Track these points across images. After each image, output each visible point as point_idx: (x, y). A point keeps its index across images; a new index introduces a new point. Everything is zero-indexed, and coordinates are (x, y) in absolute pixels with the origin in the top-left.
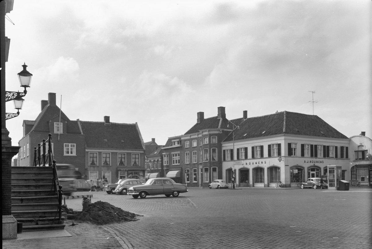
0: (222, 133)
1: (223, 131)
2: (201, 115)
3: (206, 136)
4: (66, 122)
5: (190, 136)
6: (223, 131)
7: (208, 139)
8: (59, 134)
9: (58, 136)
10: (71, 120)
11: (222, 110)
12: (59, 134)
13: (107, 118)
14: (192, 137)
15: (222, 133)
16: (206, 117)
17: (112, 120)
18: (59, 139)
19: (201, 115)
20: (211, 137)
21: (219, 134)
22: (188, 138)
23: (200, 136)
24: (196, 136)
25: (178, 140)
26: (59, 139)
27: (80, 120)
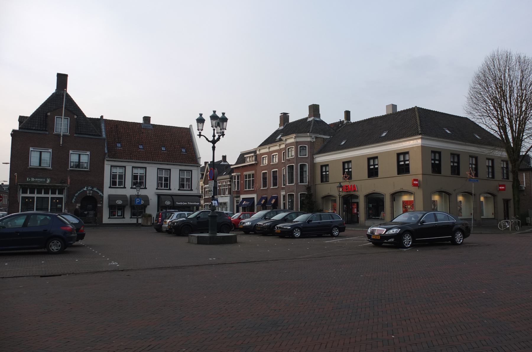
0: (314, 140)
1: (316, 138)
2: (284, 117)
3: (291, 144)
4: (75, 117)
5: (269, 148)
6: (316, 138)
7: (294, 149)
8: (62, 135)
9: (60, 137)
10: (87, 117)
11: (314, 109)
12: (62, 135)
13: (147, 119)
14: (272, 149)
15: (314, 140)
16: (291, 120)
17: (152, 122)
18: (61, 143)
19: (284, 117)
20: (299, 146)
21: (311, 142)
22: (266, 150)
23: (283, 146)
24: (277, 148)
25: (253, 154)
26: (61, 143)
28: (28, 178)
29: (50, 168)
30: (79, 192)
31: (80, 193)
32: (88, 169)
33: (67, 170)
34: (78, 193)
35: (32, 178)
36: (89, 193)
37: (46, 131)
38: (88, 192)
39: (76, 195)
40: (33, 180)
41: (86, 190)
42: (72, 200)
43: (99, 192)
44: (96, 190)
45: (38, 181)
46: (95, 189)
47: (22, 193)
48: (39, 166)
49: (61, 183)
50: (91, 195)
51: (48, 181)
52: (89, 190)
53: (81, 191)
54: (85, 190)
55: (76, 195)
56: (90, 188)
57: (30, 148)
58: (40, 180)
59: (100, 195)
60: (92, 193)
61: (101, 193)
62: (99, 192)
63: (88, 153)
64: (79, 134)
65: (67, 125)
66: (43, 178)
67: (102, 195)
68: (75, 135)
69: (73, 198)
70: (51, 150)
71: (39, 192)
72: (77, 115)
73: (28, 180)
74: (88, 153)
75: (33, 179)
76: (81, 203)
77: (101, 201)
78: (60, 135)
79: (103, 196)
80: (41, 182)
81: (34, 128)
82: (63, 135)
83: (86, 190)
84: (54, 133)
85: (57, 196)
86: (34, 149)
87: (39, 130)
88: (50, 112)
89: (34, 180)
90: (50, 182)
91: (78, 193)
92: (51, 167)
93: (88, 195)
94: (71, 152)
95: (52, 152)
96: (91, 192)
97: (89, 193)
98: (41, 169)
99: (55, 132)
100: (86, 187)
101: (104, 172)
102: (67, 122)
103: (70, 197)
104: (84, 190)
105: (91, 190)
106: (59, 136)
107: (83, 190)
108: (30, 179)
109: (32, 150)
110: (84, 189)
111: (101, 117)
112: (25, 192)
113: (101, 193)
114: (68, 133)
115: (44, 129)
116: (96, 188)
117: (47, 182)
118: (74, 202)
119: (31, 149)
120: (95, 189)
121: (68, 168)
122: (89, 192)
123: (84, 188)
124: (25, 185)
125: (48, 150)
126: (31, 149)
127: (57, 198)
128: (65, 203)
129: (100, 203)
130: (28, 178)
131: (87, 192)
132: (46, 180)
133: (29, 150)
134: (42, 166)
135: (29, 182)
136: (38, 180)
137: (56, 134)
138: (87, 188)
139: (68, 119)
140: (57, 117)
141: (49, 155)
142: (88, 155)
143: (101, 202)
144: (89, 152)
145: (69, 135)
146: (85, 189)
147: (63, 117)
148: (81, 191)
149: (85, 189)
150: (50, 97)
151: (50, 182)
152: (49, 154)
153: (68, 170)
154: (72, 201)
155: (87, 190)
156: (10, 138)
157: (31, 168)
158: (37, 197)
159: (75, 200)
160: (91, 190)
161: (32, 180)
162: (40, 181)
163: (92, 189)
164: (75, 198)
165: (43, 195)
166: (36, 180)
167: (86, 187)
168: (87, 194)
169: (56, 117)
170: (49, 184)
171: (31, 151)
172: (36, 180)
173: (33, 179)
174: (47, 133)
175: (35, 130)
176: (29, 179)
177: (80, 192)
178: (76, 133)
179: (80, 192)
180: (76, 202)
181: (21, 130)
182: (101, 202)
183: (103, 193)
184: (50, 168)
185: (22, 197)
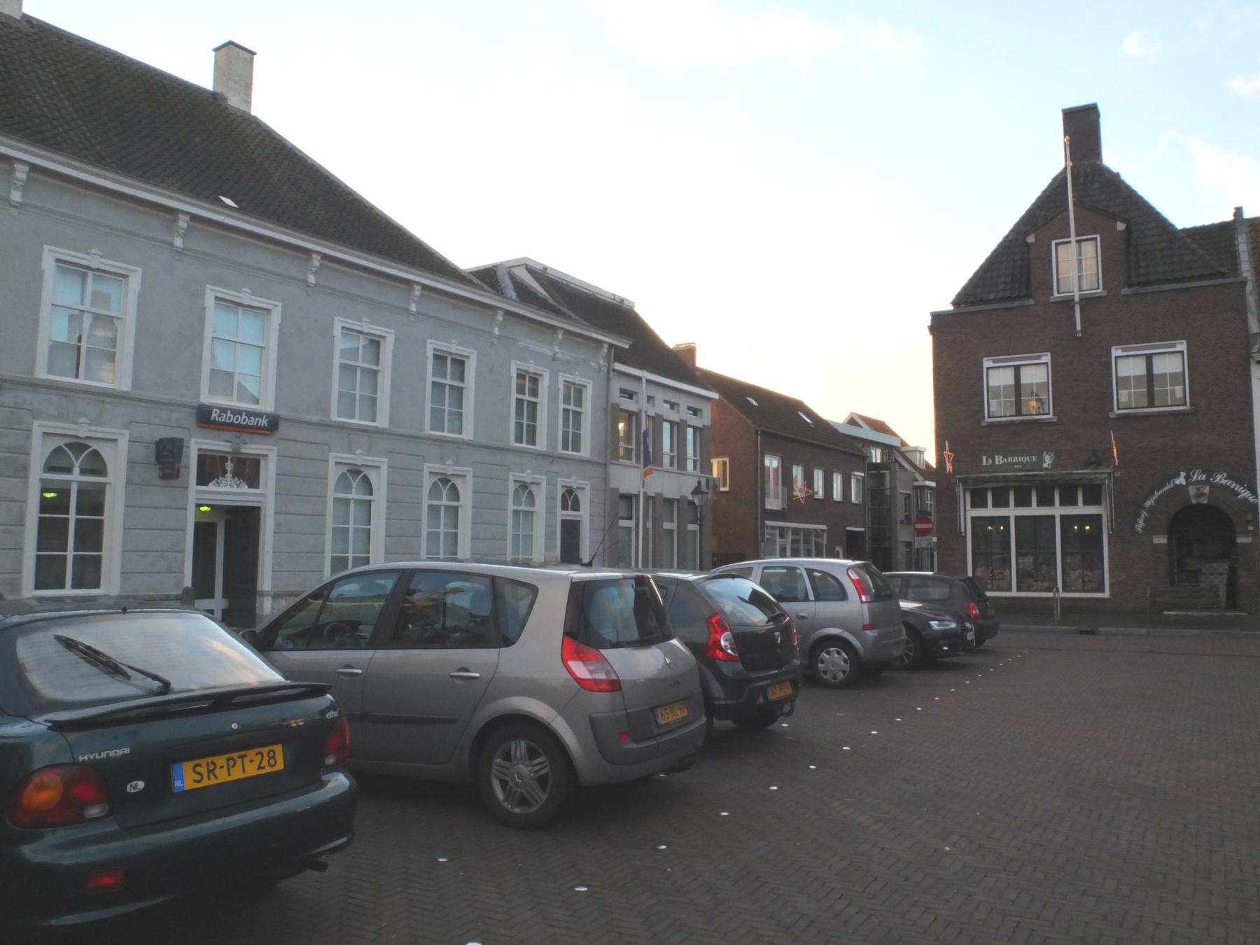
8: (1077, 299)
9: (1073, 309)
12: (1077, 299)
18: (1079, 327)
26: (1079, 327)
27: (1248, 214)
28: (984, 458)
29: (1051, 416)
30: (1157, 494)
31: (1162, 495)
32: (1185, 404)
33: (1108, 418)
34: (1154, 498)
35: (997, 457)
36: (1199, 494)
37: (1028, 296)
38: (1192, 491)
39: (1148, 504)
40: (1001, 462)
41: (1184, 483)
42: (1135, 522)
43: (1238, 488)
44: (1223, 482)
45: (1017, 464)
46: (1220, 478)
47: (974, 505)
48: (1016, 416)
49: (1088, 464)
50: (1205, 502)
51: (1048, 460)
52: (1197, 482)
53: (1165, 489)
54: (1181, 484)
55: (1148, 504)
56: (1198, 476)
57: (985, 359)
58: (1021, 459)
59: (1245, 500)
60: (1211, 492)
61: (1245, 494)
62: (1238, 488)
63: (1182, 346)
64: (1139, 284)
65: (1094, 260)
66: (1030, 454)
67: (1251, 499)
68: (1126, 291)
69: (1139, 515)
70: (1047, 358)
71: (1023, 501)
72: (1124, 221)
73: (984, 464)
74: (1182, 346)
75: (999, 460)
76: (1170, 532)
77: (1249, 522)
78: (1073, 300)
79: (1257, 504)
80: (1025, 467)
81: (992, 296)
82: (1080, 299)
83: (1184, 483)
84: (1051, 300)
85: (1081, 509)
86: (995, 361)
87: (1010, 299)
88: (1033, 232)
89: (1004, 463)
90: (1052, 464)
91: (1154, 498)
92: (1054, 414)
93: (1194, 501)
94: (1116, 352)
95: (1052, 364)
96: (1207, 490)
97: (1199, 496)
98: (1022, 423)
99: (1056, 295)
100: (1183, 474)
101: (1251, 410)
102: (1094, 253)
103: (1125, 511)
104: (1176, 486)
105: (1206, 482)
106: (1068, 303)
107: (1172, 485)
108: (990, 461)
109: (989, 366)
110: (1178, 482)
111: (1235, 215)
112: (979, 502)
113: (1245, 494)
114: (1100, 290)
115: (1023, 292)
116: (1225, 476)
117: (1045, 465)
118: (1143, 528)
119: (987, 363)
120: (1219, 477)
121: (1112, 410)
122: (1198, 489)
123: (1178, 476)
124: (977, 480)
125: (1039, 358)
126: (987, 363)
127: (1083, 519)
128: (1109, 534)
129: (1247, 533)
130: (984, 458)
131: (1189, 494)
132: (1041, 460)
133: (982, 368)
134: (1023, 413)
135: (987, 469)
136: (1015, 459)
137: (1059, 300)
138: (1187, 478)
139: (1095, 239)
140: (1057, 244)
141: (1046, 370)
142: (1182, 352)
143: (1251, 528)
144: (1185, 342)
145: (1105, 293)
146: (1181, 480)
147: (1073, 238)
148: (1165, 489)
149: (1181, 480)
150: (1045, 192)
151: (1055, 465)
152: (1043, 370)
153: (1111, 416)
154: (1134, 524)
155: (1188, 484)
156: (928, 340)
157: (990, 425)
158: (1017, 518)
159: (1144, 522)
160: (1206, 482)
161: (997, 463)
162: (1021, 463)
163: (1208, 478)
164: (1144, 514)
165: (1034, 510)
166: (1010, 460)
167: (1183, 474)
168: (1189, 497)
169: (1053, 243)
170: (1050, 470)
171: (988, 369)
172: (1010, 460)
173: (999, 460)
174: (1031, 302)
175: (995, 301)
176: (987, 461)
177: (1161, 492)
178: (1130, 285)
179: (1161, 492)
180: (1150, 530)
181: (963, 308)
182: (1251, 528)
183: (1254, 492)
184: (1051, 416)
185: (973, 519)
